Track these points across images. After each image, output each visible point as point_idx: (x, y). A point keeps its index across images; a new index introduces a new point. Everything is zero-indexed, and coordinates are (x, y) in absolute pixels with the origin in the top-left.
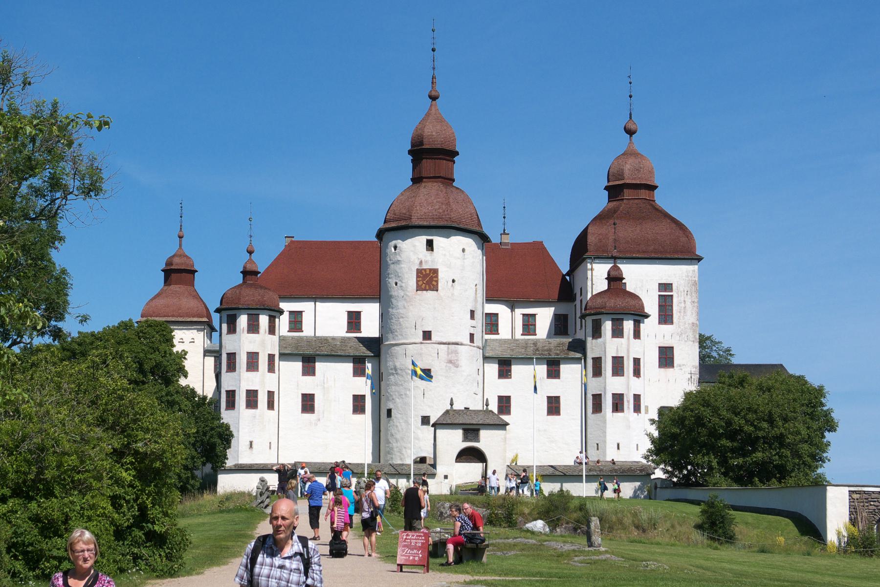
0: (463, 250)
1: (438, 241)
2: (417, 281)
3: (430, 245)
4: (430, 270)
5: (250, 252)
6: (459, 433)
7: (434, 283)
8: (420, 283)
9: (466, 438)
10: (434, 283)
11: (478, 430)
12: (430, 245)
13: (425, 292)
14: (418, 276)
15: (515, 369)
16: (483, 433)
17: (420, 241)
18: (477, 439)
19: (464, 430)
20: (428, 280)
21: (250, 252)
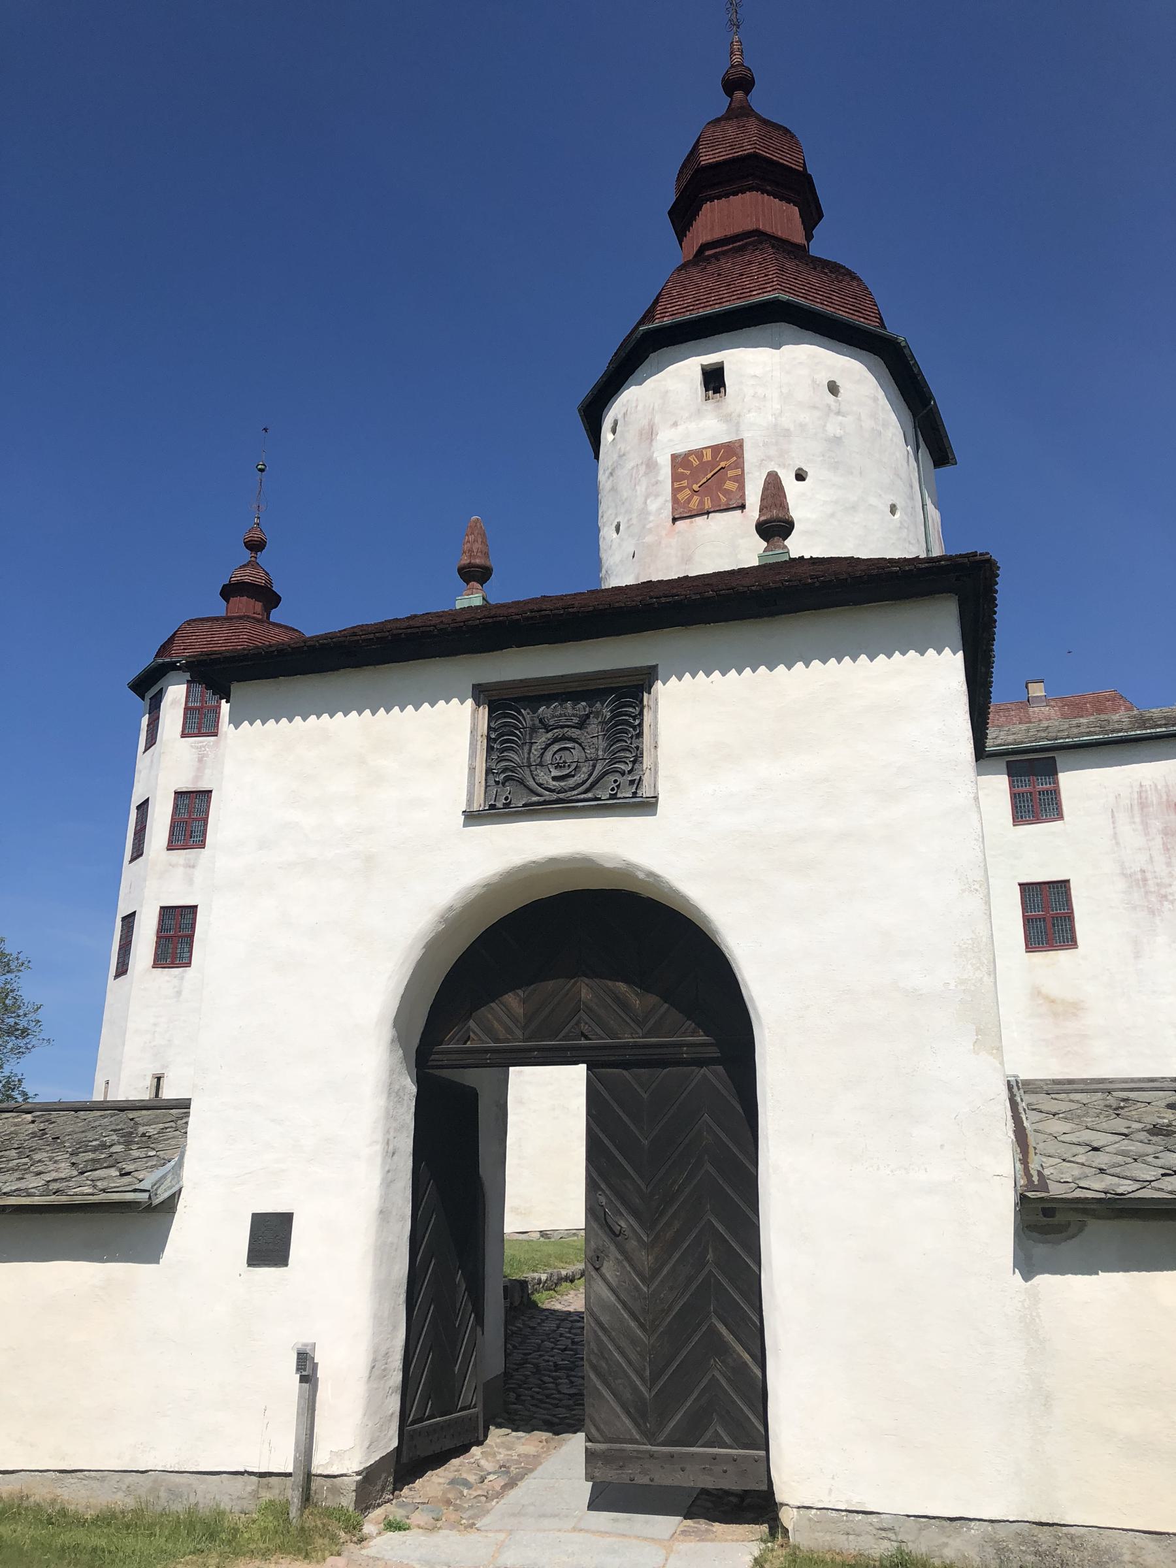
0: (833, 388)
1: (745, 362)
2: (675, 491)
3: (714, 380)
4: (715, 449)
5: (255, 546)
6: (436, 736)
7: (730, 485)
8: (683, 496)
9: (510, 786)
10: (730, 485)
11: (628, 694)
12: (714, 380)
13: (699, 520)
14: (676, 477)
15: (1077, 784)
16: (695, 712)
17: (680, 376)
18: (616, 779)
19: (499, 702)
20: (707, 479)
21: (255, 546)
